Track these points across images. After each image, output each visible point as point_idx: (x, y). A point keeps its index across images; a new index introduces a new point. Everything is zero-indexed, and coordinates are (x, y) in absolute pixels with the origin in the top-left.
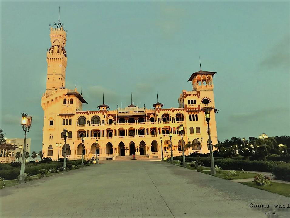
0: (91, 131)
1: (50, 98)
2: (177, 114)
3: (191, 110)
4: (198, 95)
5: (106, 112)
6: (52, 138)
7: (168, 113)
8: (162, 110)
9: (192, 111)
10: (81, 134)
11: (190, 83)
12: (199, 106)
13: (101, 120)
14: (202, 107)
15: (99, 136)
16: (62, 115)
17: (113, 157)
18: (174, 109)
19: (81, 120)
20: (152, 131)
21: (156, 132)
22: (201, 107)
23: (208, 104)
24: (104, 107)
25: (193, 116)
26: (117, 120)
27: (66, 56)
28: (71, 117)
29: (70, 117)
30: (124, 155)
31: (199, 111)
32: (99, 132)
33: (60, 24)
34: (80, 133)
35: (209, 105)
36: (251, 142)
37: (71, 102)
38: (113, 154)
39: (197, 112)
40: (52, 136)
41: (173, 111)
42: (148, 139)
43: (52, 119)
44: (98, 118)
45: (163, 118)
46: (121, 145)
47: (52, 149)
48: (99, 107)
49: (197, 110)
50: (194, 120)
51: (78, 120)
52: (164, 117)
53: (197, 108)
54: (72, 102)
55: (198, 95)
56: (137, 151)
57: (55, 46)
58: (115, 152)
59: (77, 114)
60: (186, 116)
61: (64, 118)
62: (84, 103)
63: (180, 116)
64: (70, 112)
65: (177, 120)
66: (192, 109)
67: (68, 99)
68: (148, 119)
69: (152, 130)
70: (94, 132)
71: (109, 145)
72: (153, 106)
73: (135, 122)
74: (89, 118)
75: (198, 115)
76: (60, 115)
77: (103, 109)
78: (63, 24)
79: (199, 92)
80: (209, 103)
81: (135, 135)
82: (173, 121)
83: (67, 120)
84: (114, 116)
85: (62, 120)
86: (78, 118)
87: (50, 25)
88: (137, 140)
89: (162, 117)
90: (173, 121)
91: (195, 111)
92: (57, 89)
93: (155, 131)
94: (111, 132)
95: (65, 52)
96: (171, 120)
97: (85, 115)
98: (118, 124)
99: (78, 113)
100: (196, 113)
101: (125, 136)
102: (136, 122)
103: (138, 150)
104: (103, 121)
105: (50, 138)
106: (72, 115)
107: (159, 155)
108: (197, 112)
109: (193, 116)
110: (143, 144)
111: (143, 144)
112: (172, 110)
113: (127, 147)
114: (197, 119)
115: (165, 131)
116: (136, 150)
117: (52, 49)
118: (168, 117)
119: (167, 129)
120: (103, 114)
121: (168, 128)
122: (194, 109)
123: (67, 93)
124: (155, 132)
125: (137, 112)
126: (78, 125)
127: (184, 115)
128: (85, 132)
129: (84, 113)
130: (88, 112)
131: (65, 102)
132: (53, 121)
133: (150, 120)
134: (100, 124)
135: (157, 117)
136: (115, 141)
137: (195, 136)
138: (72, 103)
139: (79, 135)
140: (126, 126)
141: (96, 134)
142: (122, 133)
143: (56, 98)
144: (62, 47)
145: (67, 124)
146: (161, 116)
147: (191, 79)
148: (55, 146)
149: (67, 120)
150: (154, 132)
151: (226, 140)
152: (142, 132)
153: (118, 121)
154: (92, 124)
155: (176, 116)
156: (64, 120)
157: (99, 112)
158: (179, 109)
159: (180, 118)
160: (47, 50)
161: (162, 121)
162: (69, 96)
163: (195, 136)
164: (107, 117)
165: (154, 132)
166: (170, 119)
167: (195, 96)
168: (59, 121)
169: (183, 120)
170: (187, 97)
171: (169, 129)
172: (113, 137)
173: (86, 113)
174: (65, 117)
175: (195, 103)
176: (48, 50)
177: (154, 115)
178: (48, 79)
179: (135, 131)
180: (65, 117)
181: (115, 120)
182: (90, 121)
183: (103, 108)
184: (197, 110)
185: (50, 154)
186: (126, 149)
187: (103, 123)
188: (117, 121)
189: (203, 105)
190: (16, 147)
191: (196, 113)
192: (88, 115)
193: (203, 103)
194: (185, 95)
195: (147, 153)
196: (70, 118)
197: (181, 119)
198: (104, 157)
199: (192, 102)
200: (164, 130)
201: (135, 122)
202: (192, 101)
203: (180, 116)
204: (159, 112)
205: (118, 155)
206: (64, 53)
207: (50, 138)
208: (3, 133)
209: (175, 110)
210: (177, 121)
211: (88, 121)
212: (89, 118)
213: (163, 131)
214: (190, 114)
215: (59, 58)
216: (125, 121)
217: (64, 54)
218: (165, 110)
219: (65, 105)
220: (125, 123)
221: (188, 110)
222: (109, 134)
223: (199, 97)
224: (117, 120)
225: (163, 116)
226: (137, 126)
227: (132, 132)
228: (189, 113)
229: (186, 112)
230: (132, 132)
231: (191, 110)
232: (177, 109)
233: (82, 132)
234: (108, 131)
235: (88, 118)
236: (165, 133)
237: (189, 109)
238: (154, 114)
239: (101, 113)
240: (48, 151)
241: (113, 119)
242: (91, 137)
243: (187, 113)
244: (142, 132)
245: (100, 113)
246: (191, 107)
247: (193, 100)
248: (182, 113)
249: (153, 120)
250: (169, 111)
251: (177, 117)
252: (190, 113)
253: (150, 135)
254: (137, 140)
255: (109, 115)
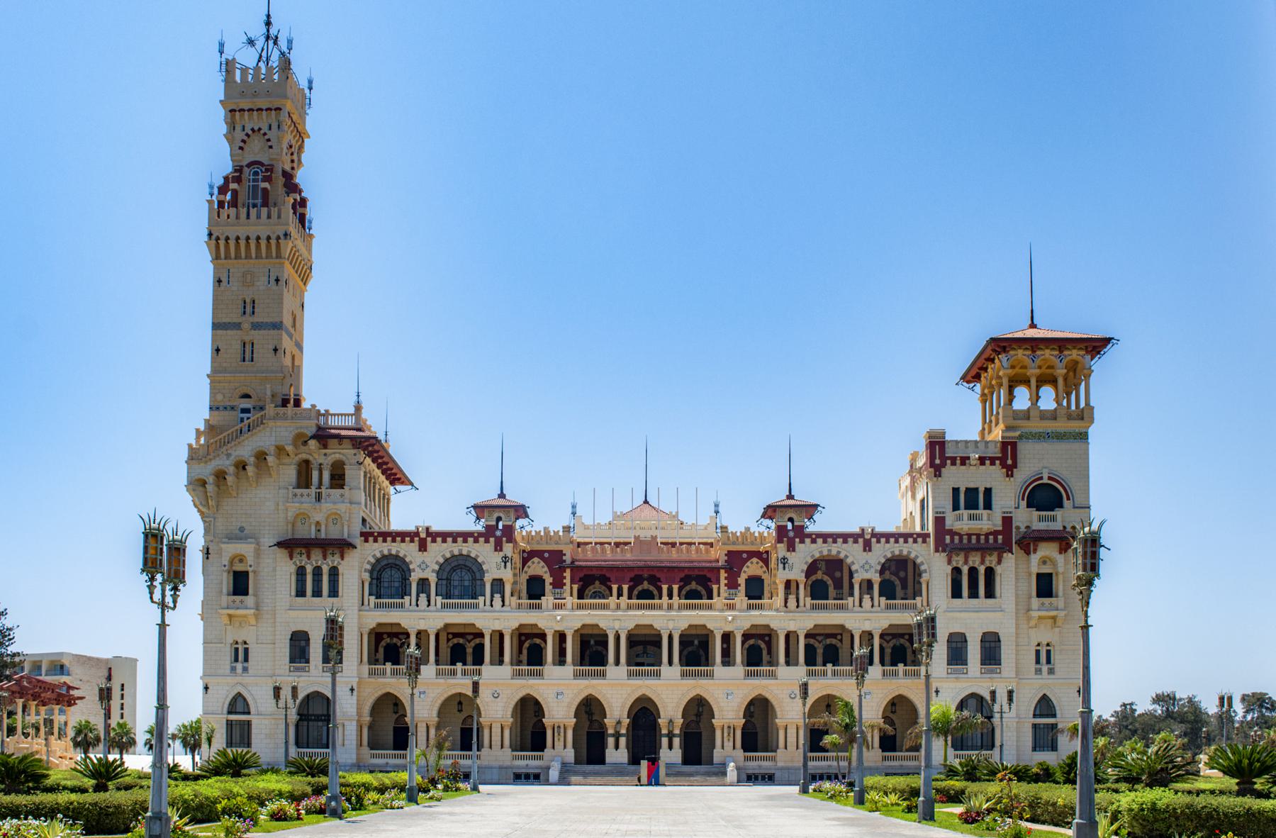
0: (437, 636)
1: (228, 455)
2: (888, 560)
3: (965, 541)
4: (1009, 462)
5: (511, 539)
6: (246, 659)
7: (842, 556)
8: (809, 535)
9: (967, 550)
10: (388, 647)
11: (971, 398)
12: (1007, 521)
13: (488, 579)
14: (1023, 529)
15: (479, 660)
16: (289, 545)
17: (548, 768)
18: (874, 535)
19: (386, 575)
20: (748, 650)
21: (769, 652)
22: (1018, 528)
23: (1058, 513)
24: (499, 519)
25: (973, 572)
26: (567, 581)
27: (304, 227)
28: (337, 559)
29: (329, 560)
30: (601, 760)
31: (1006, 547)
32: (477, 641)
33: (275, 43)
34: (383, 643)
35: (1062, 518)
36: (1249, 718)
37: (333, 477)
38: (548, 752)
39: (996, 554)
40: (246, 650)
41: (867, 547)
42: (728, 689)
43: (241, 561)
44: (470, 570)
45: (814, 578)
46: (590, 709)
47: (249, 713)
48: (480, 510)
49: (996, 540)
50: (974, 594)
51: (371, 572)
52: (819, 575)
53: (995, 533)
54: (338, 479)
55: (1009, 462)
56: (670, 747)
57: (249, 165)
58: (559, 745)
59: (366, 541)
60: (936, 570)
61: (301, 560)
62: (399, 487)
63: (902, 574)
64: (334, 533)
65: (888, 591)
66: (969, 535)
67: (323, 458)
68: (733, 585)
69: (752, 642)
70: (448, 640)
71: (529, 710)
72: (763, 516)
73: (665, 597)
74: (424, 564)
75: (998, 569)
76: (280, 544)
77: (499, 519)
78: (290, 42)
79: (1014, 445)
80: (1061, 506)
81: (660, 664)
82: (867, 598)
83: (317, 572)
84: (554, 559)
85: (293, 569)
86: (374, 566)
87: (222, 45)
88: (670, 689)
89: (807, 576)
90: (867, 598)
91: (984, 550)
92: (262, 408)
93: (763, 645)
94: (538, 641)
95: (303, 203)
96: (852, 595)
97: (408, 551)
98: (571, 600)
99: (371, 539)
100: (991, 560)
101: (611, 669)
102: (670, 596)
103: (676, 741)
104: (498, 585)
105: (236, 660)
106: (343, 546)
107: (782, 769)
108: (996, 554)
109: (973, 572)
110: (698, 710)
111: (698, 710)
112: (861, 540)
113: (619, 722)
114: (990, 594)
115: (820, 651)
116: (665, 741)
117: (233, 186)
118: (838, 574)
119: (828, 641)
120: (499, 547)
121: (834, 636)
122: (978, 536)
123: (312, 430)
124: (765, 652)
125: (673, 545)
126: (372, 598)
127: (922, 568)
128: (408, 635)
129: (403, 541)
130: (423, 535)
131: (304, 479)
132: (245, 575)
133: (742, 588)
134: (481, 599)
135: (782, 576)
136: (559, 690)
137: (974, 679)
138: (342, 487)
139: (377, 650)
140: (618, 617)
141: (463, 648)
142: (592, 649)
143: (261, 456)
144: (285, 174)
145: (317, 593)
146: (805, 567)
147: (973, 375)
148: (260, 699)
149: (317, 572)
150: (759, 650)
151: (1125, 705)
152: (696, 650)
153: (575, 587)
154: (439, 598)
155: (882, 572)
156: (301, 572)
157: (480, 534)
158: (901, 535)
159: (900, 579)
160: (207, 190)
161: (808, 599)
162: (325, 447)
163: (974, 679)
164: (519, 565)
165: (759, 650)
166: (851, 586)
167: (993, 463)
168: (276, 575)
169: (917, 593)
170: (949, 471)
171: (841, 641)
172: (550, 669)
173: (412, 541)
174: (309, 557)
175: (988, 506)
176: (211, 187)
177: (766, 562)
178: (218, 350)
179: (658, 644)
180: (309, 557)
181: (558, 584)
182: (433, 579)
183: (496, 515)
184: (996, 540)
185: (236, 737)
186: (611, 731)
187: (497, 596)
188: (567, 588)
189: (1026, 518)
190: (75, 693)
191: (988, 558)
192: (423, 547)
193: (1028, 506)
194: (938, 461)
195: (718, 754)
196: (334, 560)
197: (904, 587)
198: (501, 768)
199: (973, 499)
200: (812, 641)
201: (665, 597)
202: (972, 493)
203: (902, 574)
204: (791, 547)
205: (572, 760)
206: (294, 207)
207: (236, 660)
208: (7, 622)
209: (878, 542)
210: (883, 599)
211: (423, 584)
212: (424, 564)
213: (810, 650)
214: (954, 564)
215: (269, 238)
216: (610, 589)
217: (295, 213)
218: (825, 537)
219: (305, 491)
220: (612, 600)
221: (948, 538)
222: (525, 652)
223: (1010, 470)
224: (567, 581)
225: (812, 569)
226: (670, 617)
227: (644, 648)
228: (955, 558)
229: (937, 550)
230: (644, 648)
231: (965, 541)
232: (887, 536)
233: (391, 635)
234: (520, 635)
235: (424, 566)
236: (819, 659)
237: (952, 533)
238: (764, 557)
239: (487, 541)
240: (230, 724)
241: (549, 580)
242: (437, 663)
243: (941, 558)
244: (696, 650)
245: (482, 539)
246: (962, 522)
247: (976, 490)
248: (912, 556)
249: (755, 589)
250: (845, 542)
251: (887, 575)
252: (959, 560)
253: (739, 670)
254: (670, 689)
255: (527, 557)
